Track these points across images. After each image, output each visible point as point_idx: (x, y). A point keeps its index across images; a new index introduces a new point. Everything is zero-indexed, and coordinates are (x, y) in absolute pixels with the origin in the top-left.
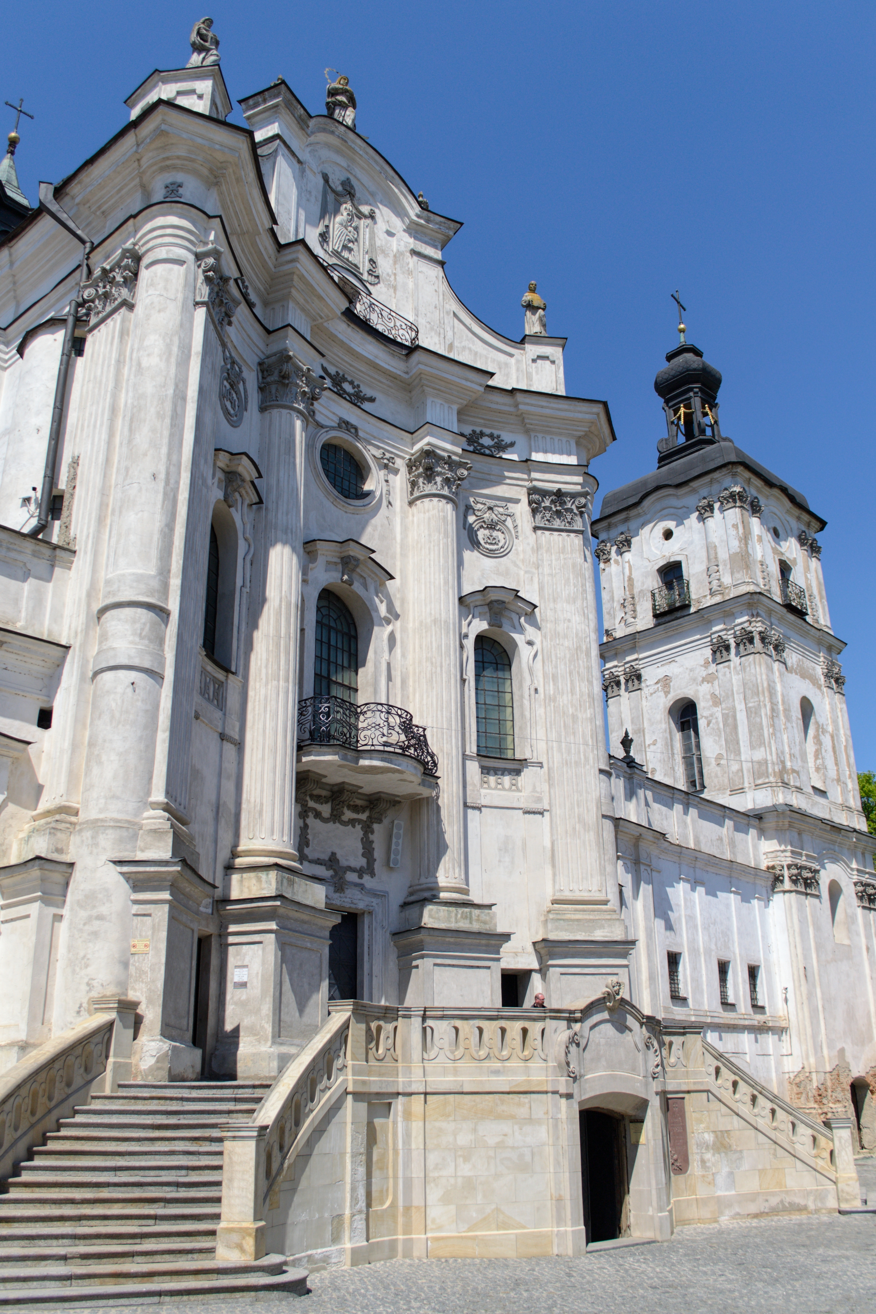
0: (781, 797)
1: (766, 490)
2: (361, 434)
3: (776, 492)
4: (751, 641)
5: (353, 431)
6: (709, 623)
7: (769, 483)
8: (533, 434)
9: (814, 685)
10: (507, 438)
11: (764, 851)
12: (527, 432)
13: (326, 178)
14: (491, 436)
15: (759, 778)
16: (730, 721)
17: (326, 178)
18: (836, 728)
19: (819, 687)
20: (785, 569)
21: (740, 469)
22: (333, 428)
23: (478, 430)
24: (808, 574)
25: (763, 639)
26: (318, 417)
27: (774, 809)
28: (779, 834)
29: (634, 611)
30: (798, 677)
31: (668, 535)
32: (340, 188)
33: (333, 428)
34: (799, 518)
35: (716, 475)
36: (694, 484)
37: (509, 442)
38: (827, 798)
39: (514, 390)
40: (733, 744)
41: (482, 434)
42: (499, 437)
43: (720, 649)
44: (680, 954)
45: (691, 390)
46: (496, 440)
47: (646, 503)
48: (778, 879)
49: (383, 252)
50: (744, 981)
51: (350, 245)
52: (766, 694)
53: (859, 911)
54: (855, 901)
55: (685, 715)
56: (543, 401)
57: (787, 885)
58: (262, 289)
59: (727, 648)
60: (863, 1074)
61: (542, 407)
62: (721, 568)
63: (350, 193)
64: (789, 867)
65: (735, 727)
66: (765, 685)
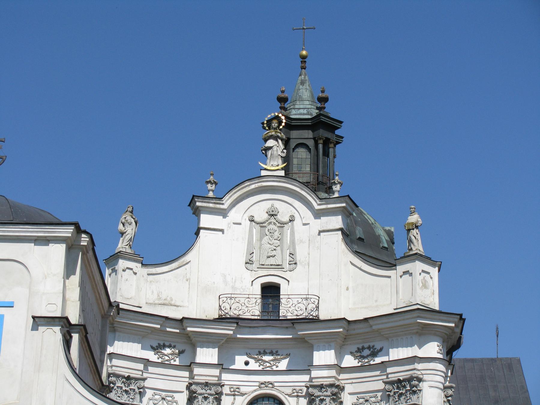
2: (276, 384)
5: (270, 386)
8: (390, 340)
10: (378, 346)
12: (387, 339)
13: (252, 220)
14: (369, 348)
17: (252, 220)
22: (255, 391)
23: (360, 346)
26: (243, 390)
32: (266, 216)
33: (255, 391)
37: (379, 348)
39: (366, 320)
41: (363, 348)
42: (373, 346)
46: (372, 350)
49: (301, 241)
51: (274, 253)
56: (385, 320)
58: (186, 341)
61: (386, 323)
63: (273, 215)
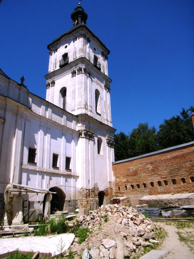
0: (83, 111)
1: (93, 37)
3: (95, 39)
4: (81, 70)
6: (72, 67)
7: (94, 36)
9: (101, 87)
11: (79, 127)
15: (79, 106)
16: (74, 92)
18: (106, 100)
19: (102, 89)
20: (96, 59)
21: (84, 28)
24: (103, 63)
25: (84, 70)
27: (81, 115)
28: (83, 122)
29: (56, 66)
30: (96, 84)
31: (66, 47)
34: (102, 49)
35: (78, 30)
36: (73, 33)
38: (101, 116)
40: (74, 98)
43: (74, 73)
44: (36, 149)
45: (79, 16)
47: (62, 39)
48: (80, 134)
50: (63, 161)
52: (84, 84)
53: (107, 146)
54: (107, 144)
55: (63, 92)
57: (83, 136)
59: (75, 73)
60: (103, 190)
62: (77, 53)
64: (84, 130)
65: (75, 93)
66: (84, 82)
